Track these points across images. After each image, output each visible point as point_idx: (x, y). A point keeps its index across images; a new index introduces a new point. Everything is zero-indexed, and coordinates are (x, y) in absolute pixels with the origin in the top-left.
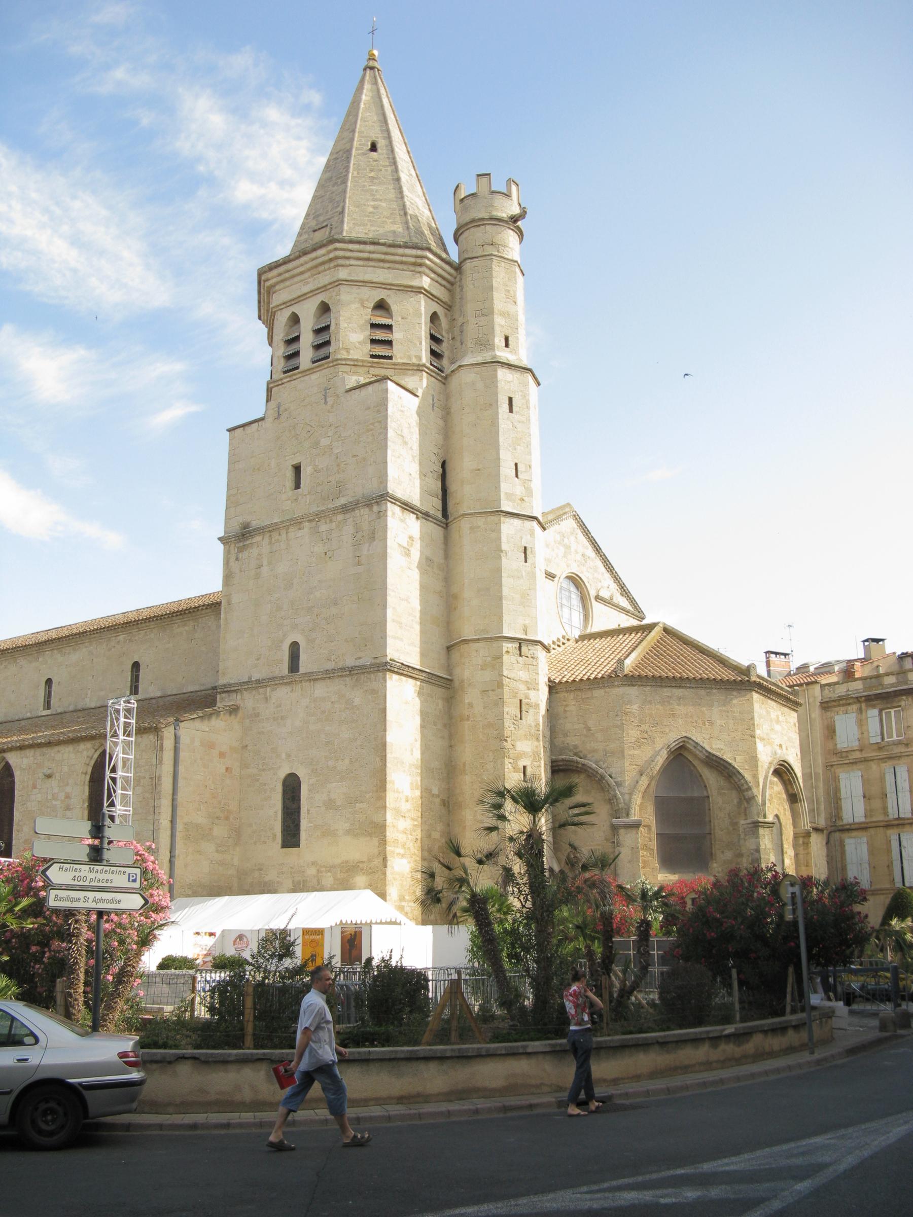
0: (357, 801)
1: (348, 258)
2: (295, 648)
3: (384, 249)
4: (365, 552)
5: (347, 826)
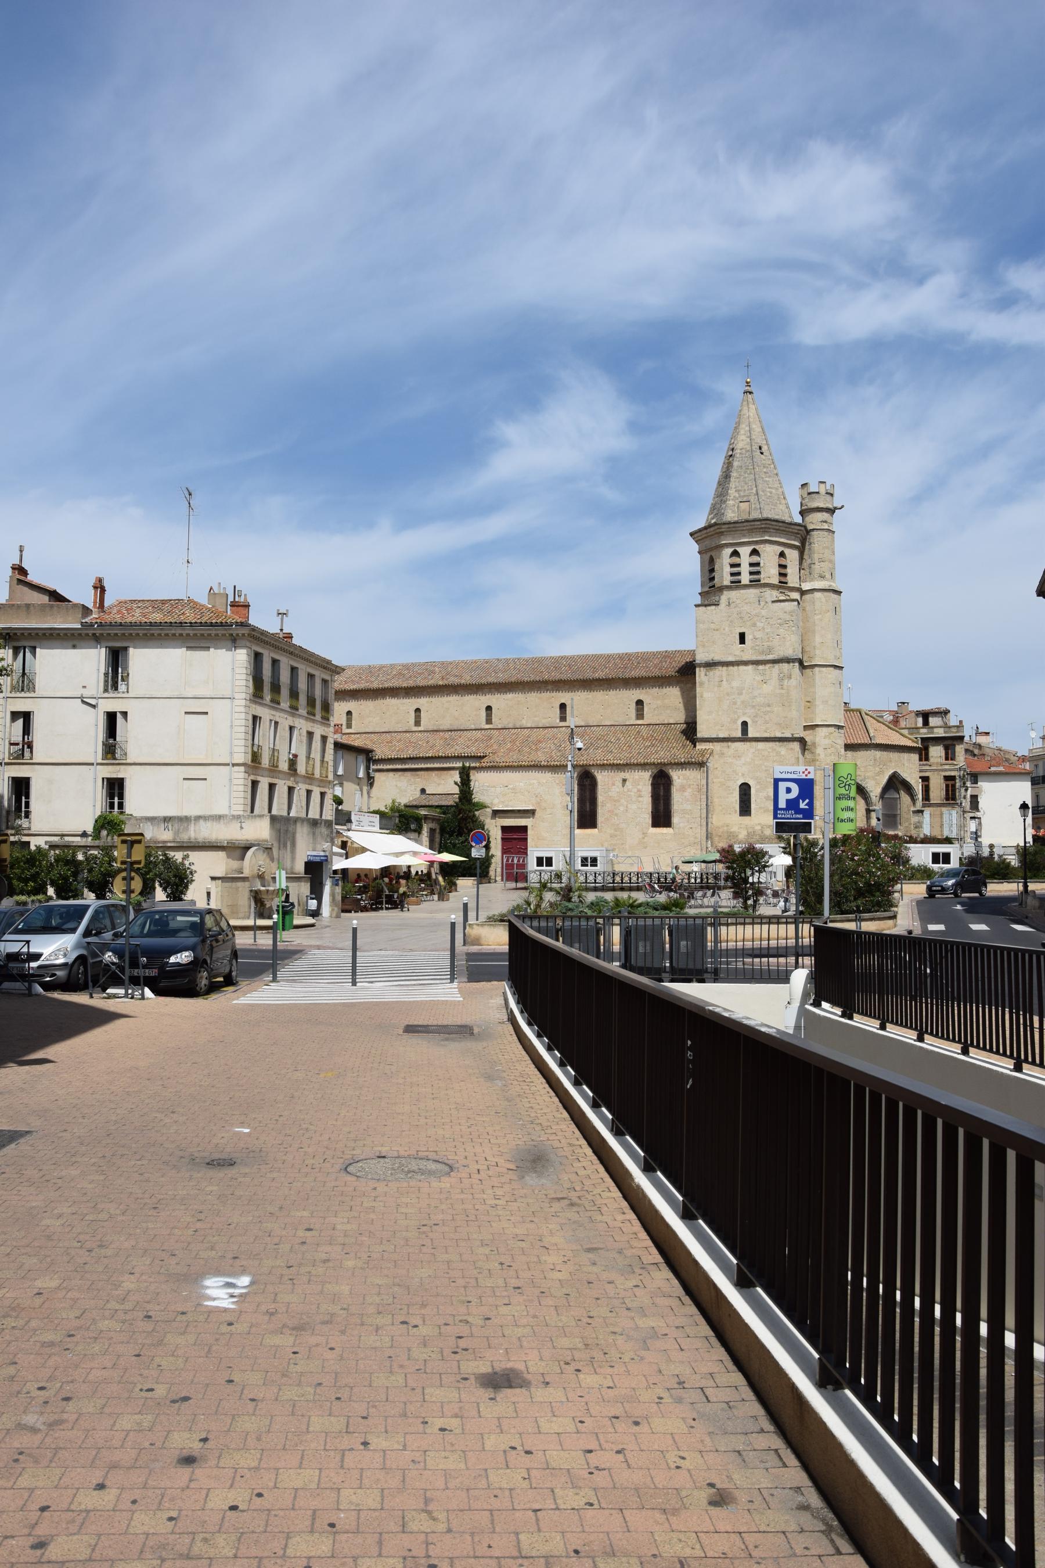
2: (745, 724)
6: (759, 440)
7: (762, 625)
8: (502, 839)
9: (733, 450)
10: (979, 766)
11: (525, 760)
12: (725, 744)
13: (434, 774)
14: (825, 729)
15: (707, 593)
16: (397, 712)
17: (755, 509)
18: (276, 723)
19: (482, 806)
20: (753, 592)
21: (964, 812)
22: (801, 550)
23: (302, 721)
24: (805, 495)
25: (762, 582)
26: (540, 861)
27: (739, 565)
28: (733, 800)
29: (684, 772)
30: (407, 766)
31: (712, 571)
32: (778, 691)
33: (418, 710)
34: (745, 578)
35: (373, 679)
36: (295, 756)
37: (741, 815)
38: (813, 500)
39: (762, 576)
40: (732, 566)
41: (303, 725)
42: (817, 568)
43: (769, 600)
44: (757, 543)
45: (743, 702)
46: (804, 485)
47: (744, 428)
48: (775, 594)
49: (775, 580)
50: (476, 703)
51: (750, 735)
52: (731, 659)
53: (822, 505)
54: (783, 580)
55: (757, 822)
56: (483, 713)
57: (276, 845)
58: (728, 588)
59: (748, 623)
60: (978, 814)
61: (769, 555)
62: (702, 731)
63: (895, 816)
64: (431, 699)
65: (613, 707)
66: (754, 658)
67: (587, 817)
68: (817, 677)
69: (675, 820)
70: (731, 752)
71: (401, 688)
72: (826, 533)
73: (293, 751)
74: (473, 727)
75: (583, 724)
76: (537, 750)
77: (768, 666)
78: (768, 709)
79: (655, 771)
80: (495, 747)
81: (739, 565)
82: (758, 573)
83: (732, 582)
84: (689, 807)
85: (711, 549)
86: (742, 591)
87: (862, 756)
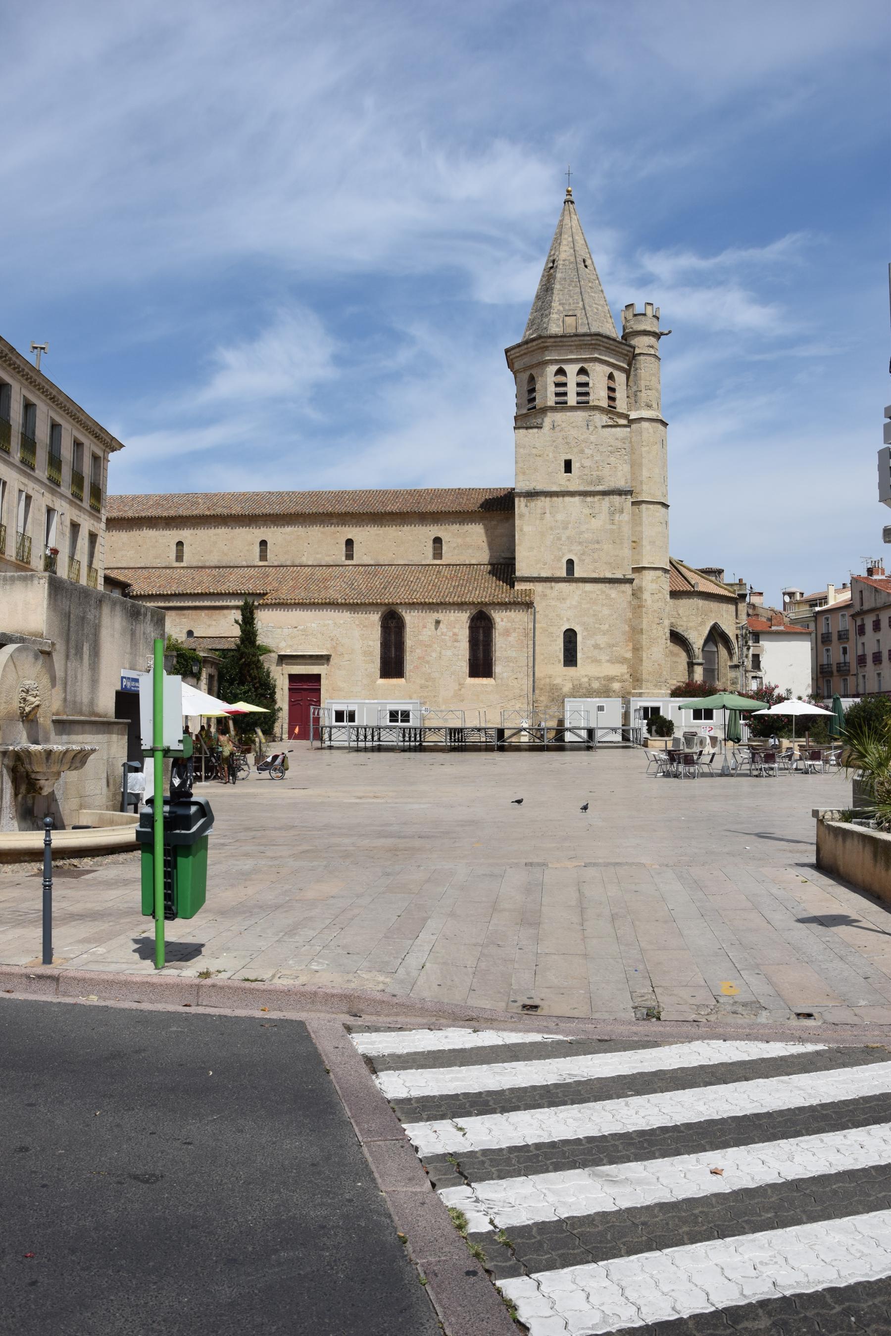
0: (613, 646)
1: (599, 345)
2: (570, 563)
3: (617, 344)
4: (617, 518)
5: (608, 658)
6: (583, 253)
7: (590, 452)
8: (290, 689)
9: (553, 262)
10: (761, 624)
11: (318, 597)
12: (548, 584)
13: (203, 613)
14: (652, 573)
15: (525, 416)
16: (157, 545)
17: (582, 324)
18: (28, 498)
19: (267, 651)
20: (580, 415)
21: (746, 671)
22: (628, 373)
23: (65, 505)
24: (630, 316)
25: (591, 404)
26: (339, 716)
27: (565, 385)
28: (557, 648)
29: (508, 613)
30: (171, 604)
31: (533, 390)
32: (609, 527)
33: (180, 544)
34: (572, 399)
35: (126, 508)
36: (55, 552)
37: (565, 666)
38: (640, 322)
39: (591, 398)
40: (557, 385)
41: (66, 511)
42: (643, 396)
43: (599, 424)
44: (585, 360)
45: (568, 538)
46: (629, 306)
47: (566, 239)
48: (604, 419)
49: (604, 403)
50: (252, 535)
51: (576, 575)
52: (555, 488)
53: (648, 328)
54: (612, 404)
55: (583, 673)
56: (257, 549)
57: (60, 647)
58: (552, 409)
59: (576, 450)
60: (759, 674)
61: (598, 374)
62: (522, 569)
63: (713, 671)
64: (196, 531)
65: (408, 544)
66: (582, 488)
67: (392, 664)
68: (644, 515)
69: (498, 669)
70: (554, 593)
71: (160, 518)
72: (653, 359)
73: (51, 544)
74: (244, 564)
75: (372, 562)
76: (326, 588)
77: (597, 498)
78: (597, 546)
79: (474, 612)
80: (275, 584)
81: (565, 385)
82: (587, 394)
83: (557, 403)
84: (514, 654)
85: (531, 367)
86: (568, 414)
87: (684, 602)
